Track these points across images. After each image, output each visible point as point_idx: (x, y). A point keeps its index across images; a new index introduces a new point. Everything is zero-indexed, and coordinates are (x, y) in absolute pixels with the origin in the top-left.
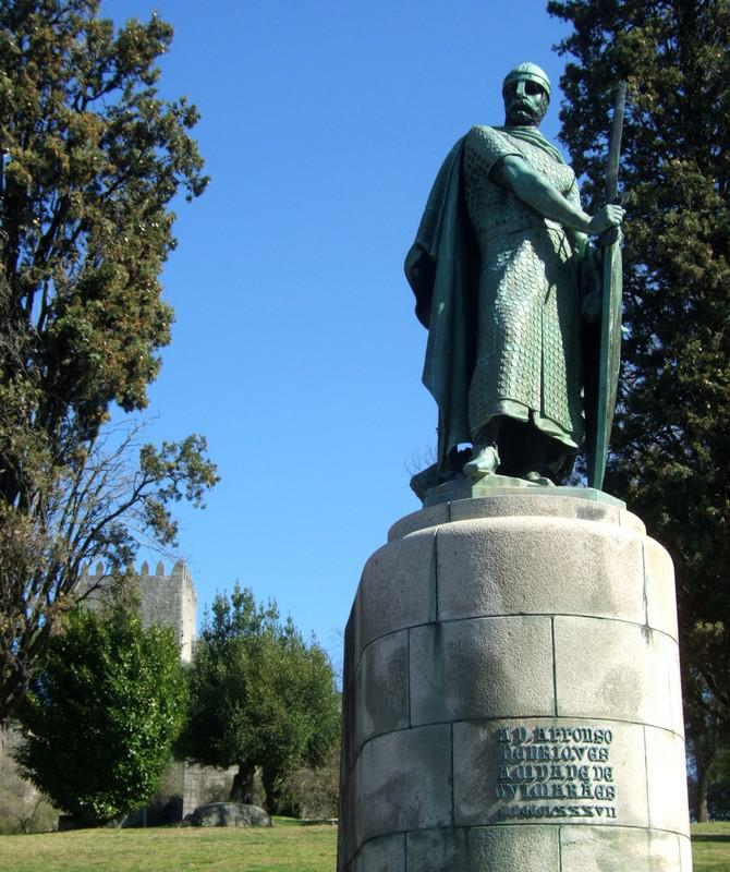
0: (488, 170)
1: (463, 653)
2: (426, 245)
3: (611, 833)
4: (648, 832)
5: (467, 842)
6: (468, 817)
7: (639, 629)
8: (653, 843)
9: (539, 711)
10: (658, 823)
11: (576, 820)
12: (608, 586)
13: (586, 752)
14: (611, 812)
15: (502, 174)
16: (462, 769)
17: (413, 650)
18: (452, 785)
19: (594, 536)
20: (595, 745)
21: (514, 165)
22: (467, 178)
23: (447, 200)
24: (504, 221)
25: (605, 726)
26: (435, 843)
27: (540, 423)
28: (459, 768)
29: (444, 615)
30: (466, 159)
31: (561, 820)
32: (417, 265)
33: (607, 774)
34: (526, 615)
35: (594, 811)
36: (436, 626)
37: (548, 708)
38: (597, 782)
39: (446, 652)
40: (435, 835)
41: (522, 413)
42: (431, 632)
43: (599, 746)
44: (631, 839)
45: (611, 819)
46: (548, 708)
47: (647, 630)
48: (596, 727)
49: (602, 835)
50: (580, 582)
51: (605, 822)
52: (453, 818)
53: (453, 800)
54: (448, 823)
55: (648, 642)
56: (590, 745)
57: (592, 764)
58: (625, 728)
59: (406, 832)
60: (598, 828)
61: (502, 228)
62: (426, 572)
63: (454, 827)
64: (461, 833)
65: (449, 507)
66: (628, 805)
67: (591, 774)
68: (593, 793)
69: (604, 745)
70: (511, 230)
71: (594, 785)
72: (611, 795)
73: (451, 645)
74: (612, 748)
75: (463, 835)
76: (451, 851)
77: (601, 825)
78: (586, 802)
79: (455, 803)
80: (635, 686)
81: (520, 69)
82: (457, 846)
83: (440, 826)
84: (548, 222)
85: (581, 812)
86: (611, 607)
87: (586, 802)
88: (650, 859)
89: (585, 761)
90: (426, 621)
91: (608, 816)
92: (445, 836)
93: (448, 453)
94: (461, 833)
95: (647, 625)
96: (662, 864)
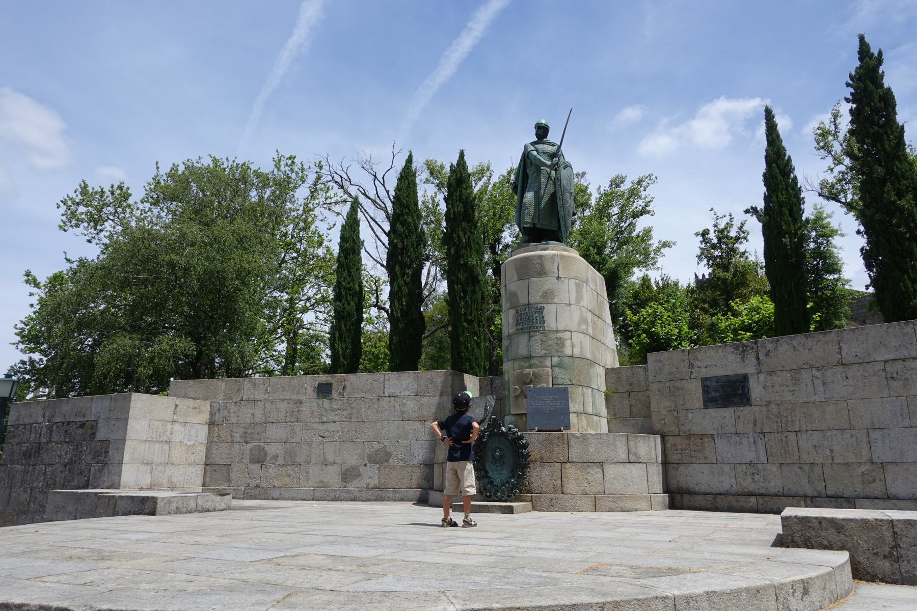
4: (557, 331)
10: (560, 328)
21: (532, 154)
25: (542, 305)
27: (539, 226)
36: (506, 286)
37: (527, 303)
40: (506, 338)
49: (542, 333)
58: (549, 305)
72: (544, 323)
84: (542, 168)
86: (546, 274)
87: (537, 325)
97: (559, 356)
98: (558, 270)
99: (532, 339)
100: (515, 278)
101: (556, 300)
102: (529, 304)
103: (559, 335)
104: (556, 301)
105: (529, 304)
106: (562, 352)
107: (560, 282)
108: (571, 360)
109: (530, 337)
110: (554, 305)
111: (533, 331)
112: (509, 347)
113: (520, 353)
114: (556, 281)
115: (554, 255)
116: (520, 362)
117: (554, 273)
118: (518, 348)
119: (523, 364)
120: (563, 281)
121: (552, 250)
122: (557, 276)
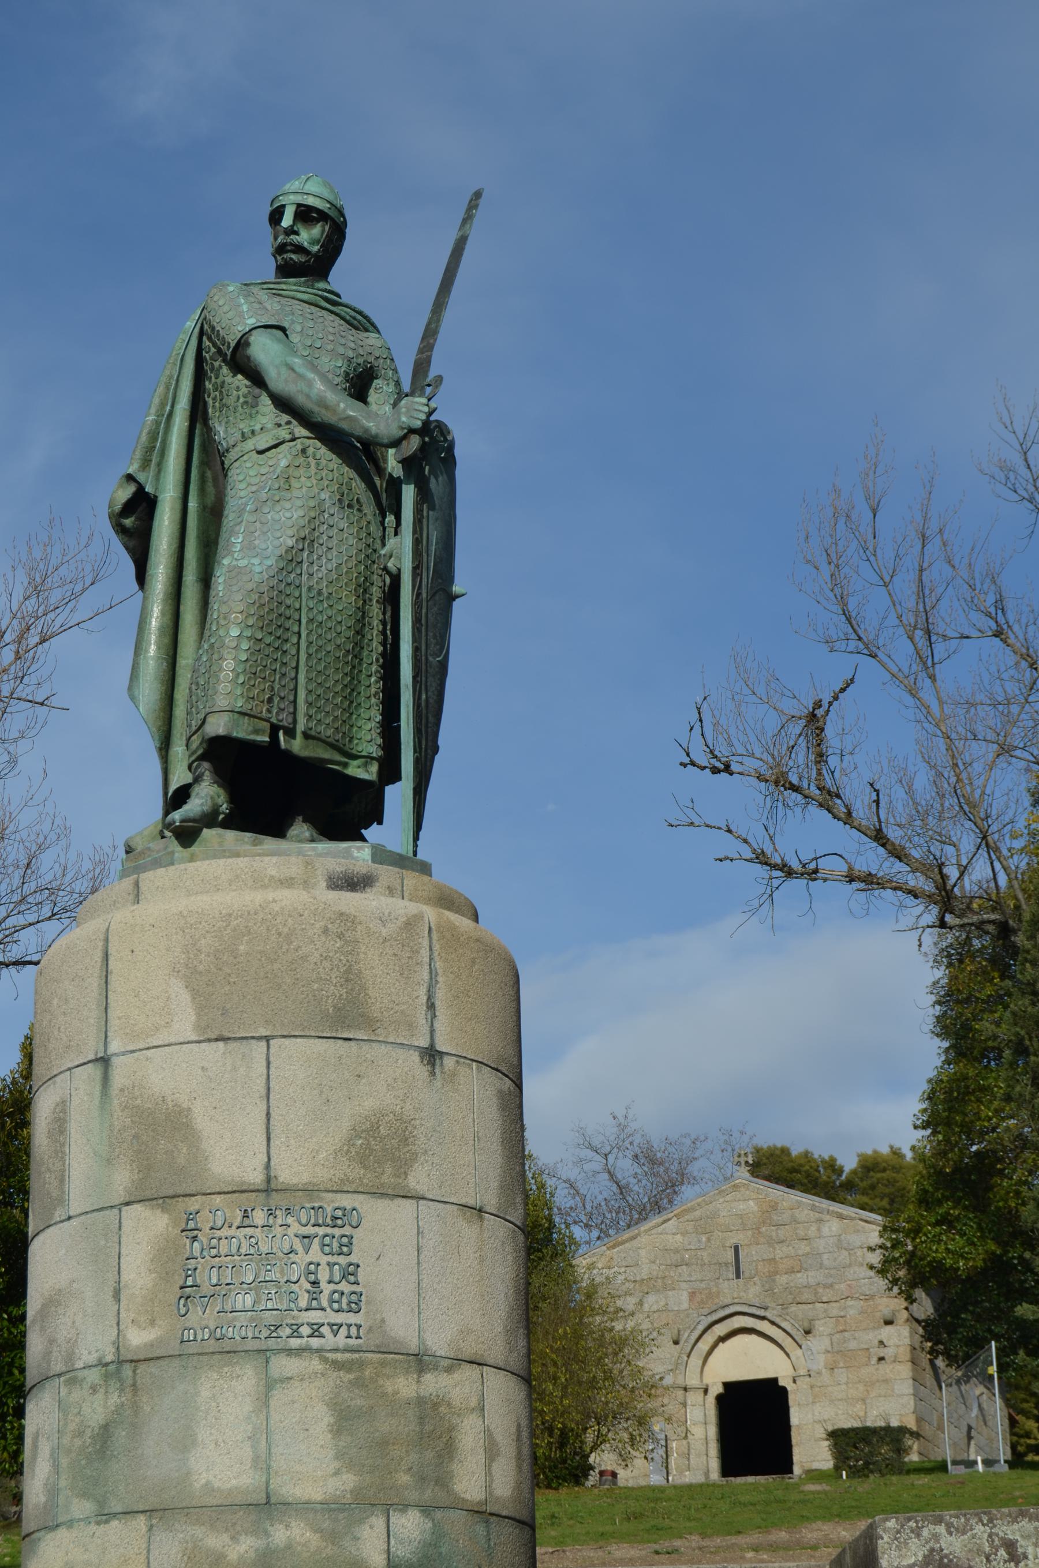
0: (229, 353)
1: (139, 1102)
2: (141, 477)
3: (352, 1362)
5: (134, 1385)
6: (138, 1347)
7: (415, 1057)
8: (428, 1377)
9: (243, 1183)
10: (439, 1343)
11: (295, 1343)
12: (363, 988)
13: (316, 1240)
14: (353, 1331)
15: (248, 358)
16: (132, 1276)
17: (76, 1101)
18: (119, 1301)
19: (342, 914)
20: (329, 1230)
22: (207, 368)
23: (173, 406)
24: (253, 432)
25: (346, 1201)
26: (94, 1389)
28: (125, 1277)
29: (114, 1047)
30: (205, 338)
31: (271, 1343)
32: (128, 508)
33: (350, 1273)
34: (229, 1039)
35: (325, 1330)
36: (104, 1061)
37: (256, 1177)
38: (332, 1287)
39: (116, 1102)
40: (94, 1376)
41: (256, 732)
42: (94, 1071)
43: (337, 1232)
44: (387, 1371)
45: (352, 1342)
46: (256, 1177)
47: (432, 1055)
48: (331, 1203)
49: (337, 1365)
50: (316, 986)
51: (341, 1346)
52: (118, 1348)
53: (118, 1324)
54: (109, 1358)
55: (433, 1073)
56: (321, 1231)
57: (324, 1260)
58: (383, 1205)
59: (59, 1375)
60: (329, 1355)
61: (250, 444)
62: (94, 983)
63: (120, 1362)
64: (127, 1371)
65: (137, 884)
66: (383, 1321)
67: (323, 1275)
68: (325, 1303)
69: (347, 1230)
70: (262, 446)
71: (327, 1288)
73: (122, 1090)
74: (357, 1234)
75: (130, 1373)
76: (114, 1399)
77: (336, 1350)
78: (315, 1316)
79: (122, 1327)
80: (405, 1141)
81: (287, 187)
82: (122, 1390)
83: (102, 1364)
85: (305, 1330)
86: (369, 1022)
87: (315, 1316)
88: (420, 1401)
89: (315, 1253)
90: (91, 1057)
91: (349, 1337)
92: (107, 1377)
93: (170, 794)
94: (127, 1371)
95: (432, 1045)
96: (443, 1409)
97: (426, 1510)
98: (431, 1006)
99: (278, 1396)
100: (184, 1025)
101: (418, 1179)
102: (269, 1187)
103: (433, 1383)
104: (422, 1189)
105: (269, 1187)
106: (443, 1481)
107: (438, 1083)
108: (480, 1529)
109: (269, 1385)
110: (410, 1204)
111: (289, 1352)
112: (121, 1435)
113: (199, 1481)
114: (421, 1071)
115: (410, 924)
116: (199, 1531)
117: (411, 1026)
118: (186, 1442)
119: (216, 1541)
120: (453, 1075)
121: (391, 891)
122: (424, 1043)
